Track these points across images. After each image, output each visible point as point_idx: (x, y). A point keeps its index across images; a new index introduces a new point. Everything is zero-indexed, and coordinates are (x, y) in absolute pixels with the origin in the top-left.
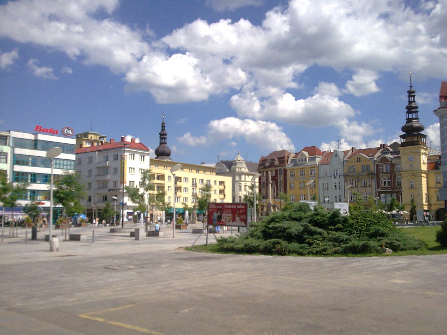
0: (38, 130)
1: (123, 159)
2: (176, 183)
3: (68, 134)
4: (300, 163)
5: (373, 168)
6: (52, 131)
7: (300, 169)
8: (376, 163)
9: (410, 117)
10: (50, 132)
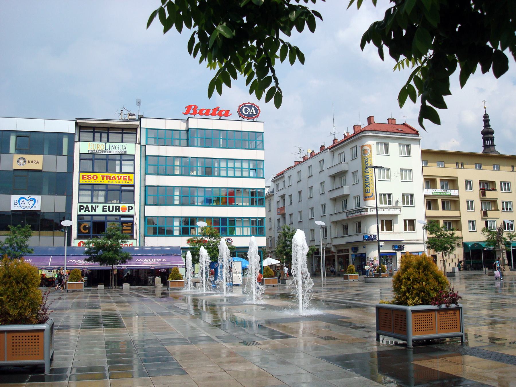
0: (192, 111)
1: (364, 152)
2: (484, 194)
3: (249, 115)
6: (217, 112)
10: (213, 114)
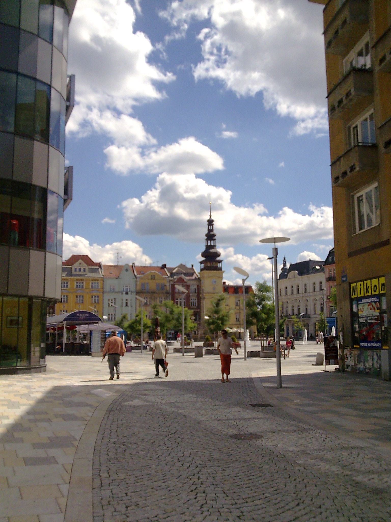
4: (75, 273)
5: (169, 288)
7: (77, 280)
8: (172, 283)
9: (209, 244)
